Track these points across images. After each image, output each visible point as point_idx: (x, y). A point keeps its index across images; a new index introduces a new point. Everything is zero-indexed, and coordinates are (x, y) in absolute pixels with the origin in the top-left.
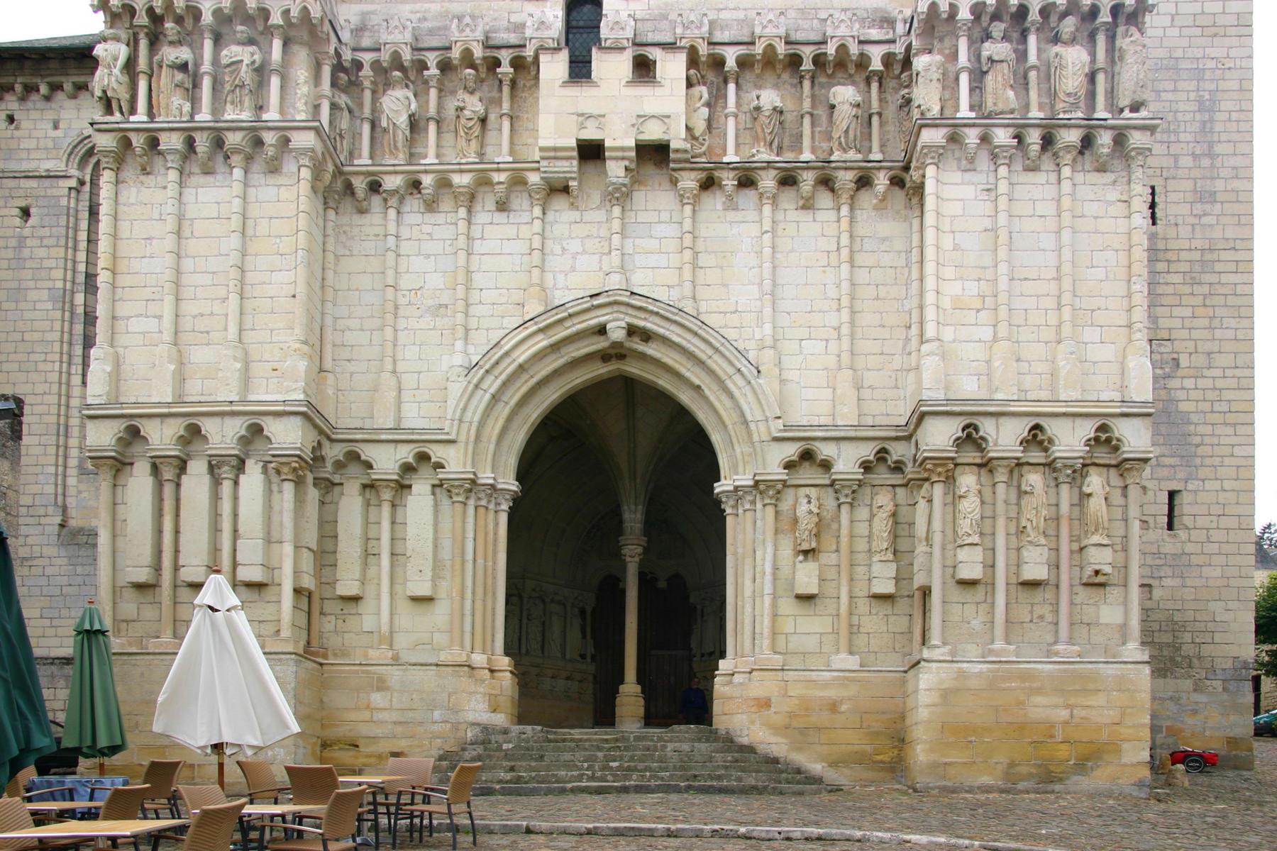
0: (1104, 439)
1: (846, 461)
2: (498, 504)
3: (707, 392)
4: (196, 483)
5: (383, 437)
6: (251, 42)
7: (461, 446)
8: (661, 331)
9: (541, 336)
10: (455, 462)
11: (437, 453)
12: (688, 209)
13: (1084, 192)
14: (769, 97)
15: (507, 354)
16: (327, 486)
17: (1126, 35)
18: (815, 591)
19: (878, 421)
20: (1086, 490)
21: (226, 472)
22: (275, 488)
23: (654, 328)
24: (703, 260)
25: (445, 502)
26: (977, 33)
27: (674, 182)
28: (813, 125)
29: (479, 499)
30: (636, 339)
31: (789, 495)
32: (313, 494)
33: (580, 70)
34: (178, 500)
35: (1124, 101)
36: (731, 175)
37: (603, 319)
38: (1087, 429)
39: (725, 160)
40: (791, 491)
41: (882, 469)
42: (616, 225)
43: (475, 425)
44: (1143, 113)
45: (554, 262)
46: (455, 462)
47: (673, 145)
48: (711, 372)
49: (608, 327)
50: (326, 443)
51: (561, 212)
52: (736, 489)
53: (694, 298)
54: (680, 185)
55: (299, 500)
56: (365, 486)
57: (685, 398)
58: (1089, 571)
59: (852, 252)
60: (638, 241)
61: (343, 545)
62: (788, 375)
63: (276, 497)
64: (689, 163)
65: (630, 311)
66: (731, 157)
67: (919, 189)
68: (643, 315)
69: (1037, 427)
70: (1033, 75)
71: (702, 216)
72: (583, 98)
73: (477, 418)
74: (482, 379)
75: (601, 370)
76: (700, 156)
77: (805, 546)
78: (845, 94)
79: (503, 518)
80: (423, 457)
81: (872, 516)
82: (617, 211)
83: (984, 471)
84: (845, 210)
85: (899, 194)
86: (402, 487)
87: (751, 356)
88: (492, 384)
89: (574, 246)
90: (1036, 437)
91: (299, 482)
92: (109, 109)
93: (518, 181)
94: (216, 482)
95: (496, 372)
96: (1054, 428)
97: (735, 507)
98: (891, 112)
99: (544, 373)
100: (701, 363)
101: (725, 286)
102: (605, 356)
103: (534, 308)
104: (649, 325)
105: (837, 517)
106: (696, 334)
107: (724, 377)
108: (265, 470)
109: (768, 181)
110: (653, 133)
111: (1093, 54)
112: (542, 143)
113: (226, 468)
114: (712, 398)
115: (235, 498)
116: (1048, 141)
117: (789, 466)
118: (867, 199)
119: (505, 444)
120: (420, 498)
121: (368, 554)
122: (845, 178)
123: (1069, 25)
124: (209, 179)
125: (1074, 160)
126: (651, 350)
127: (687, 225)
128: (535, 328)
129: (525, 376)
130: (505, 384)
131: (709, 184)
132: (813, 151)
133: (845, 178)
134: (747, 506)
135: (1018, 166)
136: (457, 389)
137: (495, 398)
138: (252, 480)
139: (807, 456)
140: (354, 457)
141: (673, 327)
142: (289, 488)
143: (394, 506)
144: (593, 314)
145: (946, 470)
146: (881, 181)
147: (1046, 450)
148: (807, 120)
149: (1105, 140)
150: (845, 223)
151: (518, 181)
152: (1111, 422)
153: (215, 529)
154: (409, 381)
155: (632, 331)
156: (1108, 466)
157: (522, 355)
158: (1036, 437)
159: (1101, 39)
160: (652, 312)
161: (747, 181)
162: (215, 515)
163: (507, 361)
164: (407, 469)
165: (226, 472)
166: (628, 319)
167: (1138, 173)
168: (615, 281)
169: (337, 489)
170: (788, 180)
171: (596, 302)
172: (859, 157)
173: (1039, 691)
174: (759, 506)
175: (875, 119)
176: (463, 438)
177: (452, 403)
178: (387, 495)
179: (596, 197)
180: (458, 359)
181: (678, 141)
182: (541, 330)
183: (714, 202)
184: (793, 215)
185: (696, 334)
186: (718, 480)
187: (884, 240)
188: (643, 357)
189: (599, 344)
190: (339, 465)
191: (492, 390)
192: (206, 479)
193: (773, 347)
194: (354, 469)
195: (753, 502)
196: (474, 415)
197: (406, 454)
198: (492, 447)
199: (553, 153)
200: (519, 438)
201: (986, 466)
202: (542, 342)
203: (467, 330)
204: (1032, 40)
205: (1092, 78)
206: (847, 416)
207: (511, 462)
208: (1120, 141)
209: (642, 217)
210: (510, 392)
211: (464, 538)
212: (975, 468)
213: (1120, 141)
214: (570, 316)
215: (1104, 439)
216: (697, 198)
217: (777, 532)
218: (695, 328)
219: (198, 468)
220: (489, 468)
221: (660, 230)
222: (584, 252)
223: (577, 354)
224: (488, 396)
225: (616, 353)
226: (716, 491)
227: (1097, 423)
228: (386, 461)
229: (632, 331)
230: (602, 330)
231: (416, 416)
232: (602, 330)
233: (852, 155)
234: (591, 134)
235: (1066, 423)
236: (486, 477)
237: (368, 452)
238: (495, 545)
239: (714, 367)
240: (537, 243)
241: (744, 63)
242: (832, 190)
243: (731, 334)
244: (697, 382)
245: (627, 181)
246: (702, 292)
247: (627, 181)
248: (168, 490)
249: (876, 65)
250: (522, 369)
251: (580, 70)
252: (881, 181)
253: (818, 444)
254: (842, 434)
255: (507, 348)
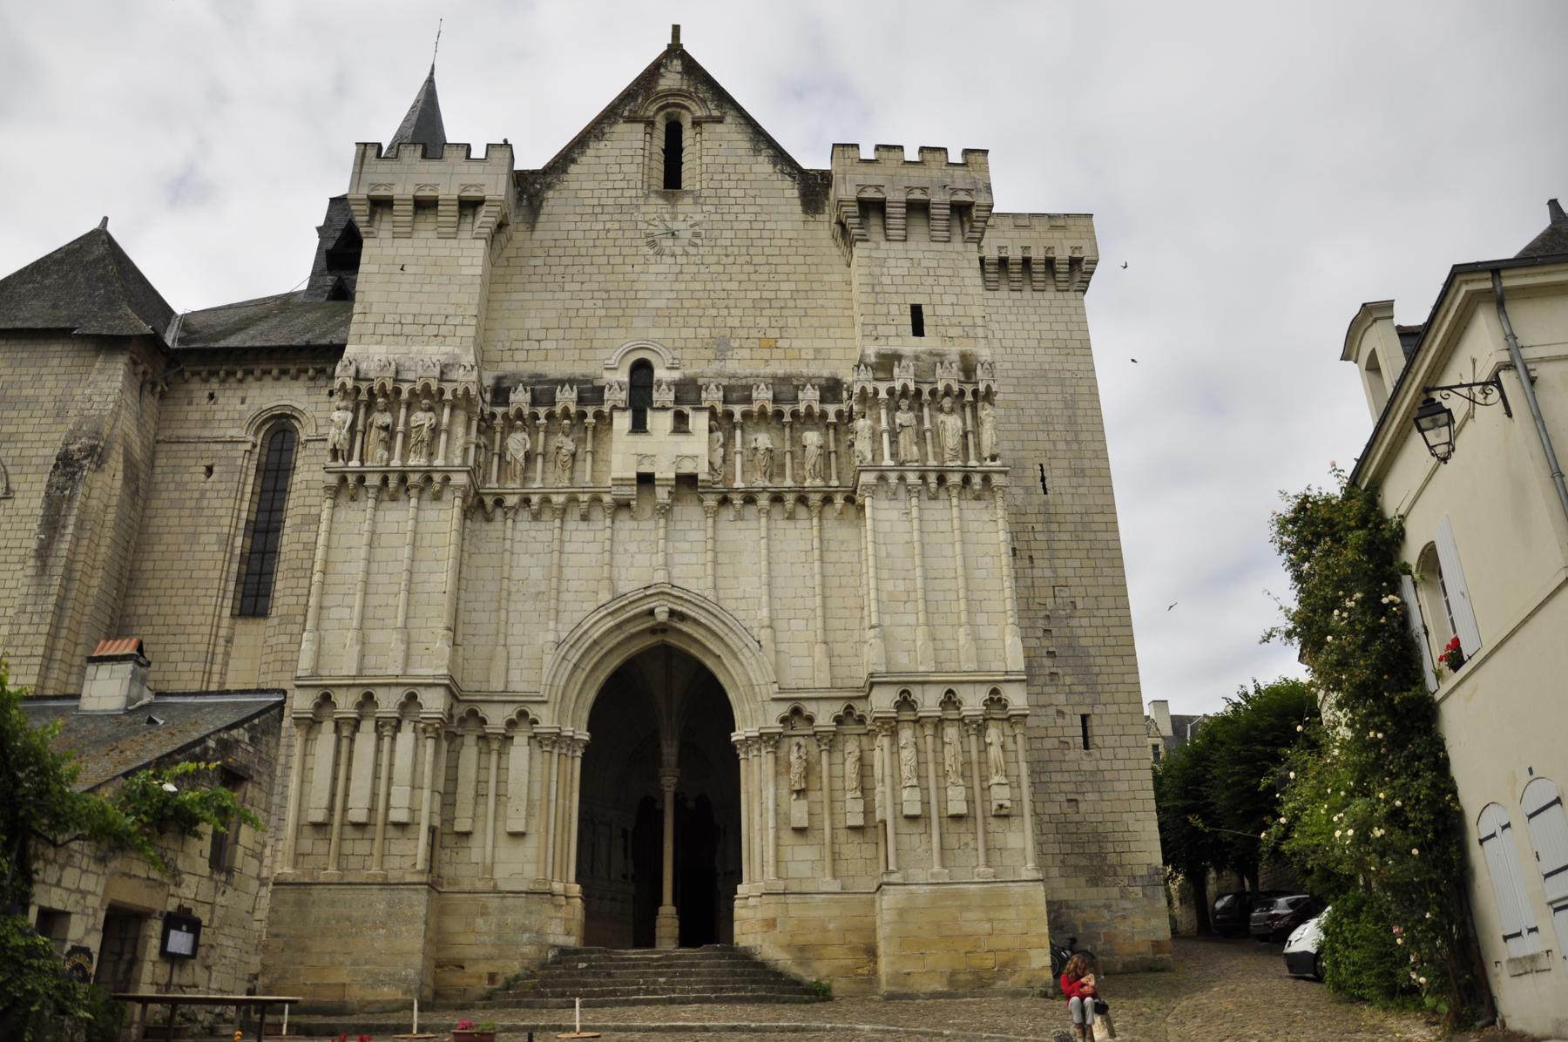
0: (995, 700)
1: (824, 716)
2: (574, 751)
3: (725, 661)
4: (365, 740)
5: (496, 698)
6: (430, 409)
7: (551, 705)
8: (693, 614)
9: (609, 618)
10: (546, 719)
11: (534, 711)
12: (710, 521)
13: (969, 514)
14: (763, 440)
15: (586, 632)
16: (452, 737)
17: (983, 408)
18: (806, 825)
19: (848, 683)
20: (988, 740)
21: (387, 731)
22: (420, 742)
23: (689, 612)
24: (722, 558)
25: (537, 751)
26: (892, 404)
27: (701, 501)
28: (792, 458)
29: (561, 748)
30: (675, 619)
31: (785, 743)
32: (445, 744)
33: (639, 426)
34: (351, 752)
35: (986, 454)
36: (739, 496)
37: (652, 605)
38: (983, 693)
39: (736, 485)
40: (786, 740)
41: (850, 721)
42: (661, 533)
43: (561, 689)
44: (998, 462)
45: (621, 560)
46: (546, 719)
47: (700, 477)
48: (727, 645)
49: (656, 611)
50: (456, 704)
51: (625, 524)
52: (747, 739)
53: (715, 588)
54: (705, 503)
55: (437, 753)
56: (479, 737)
57: (709, 663)
58: (995, 806)
59: (821, 551)
60: (677, 544)
61: (460, 789)
62: (782, 647)
63: (421, 749)
64: (709, 488)
65: (671, 599)
66: (738, 484)
67: (862, 507)
68: (680, 602)
69: (950, 691)
70: (928, 434)
71: (720, 525)
72: (641, 443)
73: (562, 683)
74: (567, 652)
75: (651, 641)
76: (718, 483)
77: (797, 787)
78: (812, 438)
79: (578, 762)
80: (523, 714)
81: (845, 760)
82: (662, 522)
83: (917, 726)
84: (815, 521)
85: (852, 510)
86: (507, 739)
87: (755, 632)
88: (574, 657)
89: (633, 547)
90: (950, 700)
91: (437, 739)
92: (335, 458)
93: (596, 500)
94: (380, 738)
95: (577, 646)
96: (962, 692)
97: (747, 753)
98: (843, 448)
99: (610, 645)
100: (721, 639)
101: (736, 578)
102: (653, 631)
103: (605, 597)
104: (684, 610)
105: (819, 761)
106: (716, 616)
107: (736, 650)
108: (415, 730)
109: (763, 501)
110: (687, 468)
111: (965, 424)
112: (614, 475)
113: (388, 728)
114: (728, 666)
115: (392, 751)
116: (941, 480)
117: (783, 720)
118: (830, 512)
119: (581, 701)
120: (519, 751)
121: (479, 795)
122: (815, 499)
123: (947, 403)
124: (394, 504)
125: (960, 493)
126: (686, 627)
127: (710, 533)
128: (605, 612)
129: (597, 648)
130: (583, 656)
131: (725, 501)
132: (794, 479)
133: (815, 499)
134: (755, 753)
135: (924, 497)
136: (548, 660)
137: (576, 666)
138: (406, 738)
139: (796, 712)
140: (473, 713)
141: (701, 611)
142: (430, 743)
143: (499, 754)
144: (645, 601)
145: (891, 727)
146: (839, 501)
147: (958, 709)
148: (788, 456)
149: (977, 479)
150: (815, 531)
151: (596, 500)
152: (999, 687)
153: (376, 777)
154: (516, 652)
155: (672, 613)
156: (1002, 720)
157: (596, 634)
158: (950, 700)
159: (968, 410)
160: (686, 600)
161: (750, 499)
162: (377, 765)
163: (586, 637)
164: (511, 724)
165: (387, 731)
166: (670, 605)
167: (1000, 503)
168: (660, 577)
169: (458, 740)
170: (777, 498)
171: (649, 592)
172: (822, 484)
173: (967, 908)
174: (763, 752)
175: (833, 455)
176: (552, 700)
177: (545, 671)
178: (495, 746)
179: (648, 510)
180: (551, 637)
181: (704, 475)
182: (609, 614)
183: (728, 514)
184: (782, 524)
185: (716, 616)
186: (734, 730)
187: (842, 542)
188: (680, 632)
189: (647, 624)
190: (462, 721)
191: (574, 661)
192: (374, 736)
193: (770, 627)
194: (471, 724)
195: (759, 750)
196: (561, 681)
197: (510, 712)
198: (572, 705)
199: (619, 482)
200: (591, 695)
201: (918, 722)
202: (610, 623)
203: (558, 612)
204: (926, 410)
205: (965, 435)
206: (823, 680)
207: (584, 715)
208: (986, 479)
209: (680, 526)
210: (585, 662)
211: (550, 781)
212: (911, 724)
213: (986, 479)
214: (631, 603)
215: (995, 700)
216: (716, 513)
217: (777, 774)
218: (715, 612)
219: (368, 726)
220: (569, 724)
221: (692, 535)
222: (640, 552)
223: (633, 631)
224: (571, 665)
225: (662, 629)
226: (733, 739)
227: (990, 687)
228: (496, 717)
229: (672, 613)
230: (651, 612)
231: (521, 682)
232: (651, 612)
233: (818, 482)
234: (646, 469)
235: (970, 688)
236: (568, 731)
237: (485, 711)
238: (571, 786)
239: (729, 642)
240: (607, 545)
241: (746, 415)
242: (807, 506)
243: (740, 615)
244: (718, 653)
245: (669, 501)
246: (721, 583)
247: (669, 501)
248: (345, 744)
249: (832, 418)
250: (595, 643)
251: (639, 426)
252: (839, 501)
253: (803, 703)
254: (820, 695)
255: (585, 628)
